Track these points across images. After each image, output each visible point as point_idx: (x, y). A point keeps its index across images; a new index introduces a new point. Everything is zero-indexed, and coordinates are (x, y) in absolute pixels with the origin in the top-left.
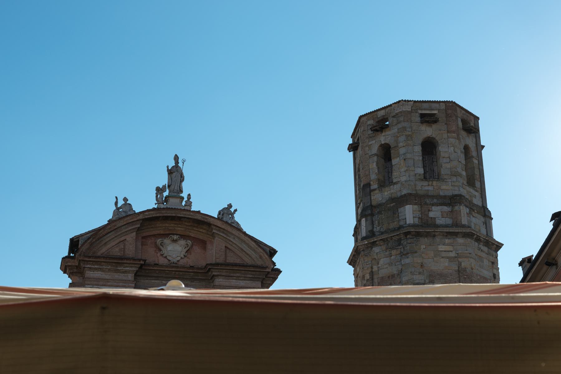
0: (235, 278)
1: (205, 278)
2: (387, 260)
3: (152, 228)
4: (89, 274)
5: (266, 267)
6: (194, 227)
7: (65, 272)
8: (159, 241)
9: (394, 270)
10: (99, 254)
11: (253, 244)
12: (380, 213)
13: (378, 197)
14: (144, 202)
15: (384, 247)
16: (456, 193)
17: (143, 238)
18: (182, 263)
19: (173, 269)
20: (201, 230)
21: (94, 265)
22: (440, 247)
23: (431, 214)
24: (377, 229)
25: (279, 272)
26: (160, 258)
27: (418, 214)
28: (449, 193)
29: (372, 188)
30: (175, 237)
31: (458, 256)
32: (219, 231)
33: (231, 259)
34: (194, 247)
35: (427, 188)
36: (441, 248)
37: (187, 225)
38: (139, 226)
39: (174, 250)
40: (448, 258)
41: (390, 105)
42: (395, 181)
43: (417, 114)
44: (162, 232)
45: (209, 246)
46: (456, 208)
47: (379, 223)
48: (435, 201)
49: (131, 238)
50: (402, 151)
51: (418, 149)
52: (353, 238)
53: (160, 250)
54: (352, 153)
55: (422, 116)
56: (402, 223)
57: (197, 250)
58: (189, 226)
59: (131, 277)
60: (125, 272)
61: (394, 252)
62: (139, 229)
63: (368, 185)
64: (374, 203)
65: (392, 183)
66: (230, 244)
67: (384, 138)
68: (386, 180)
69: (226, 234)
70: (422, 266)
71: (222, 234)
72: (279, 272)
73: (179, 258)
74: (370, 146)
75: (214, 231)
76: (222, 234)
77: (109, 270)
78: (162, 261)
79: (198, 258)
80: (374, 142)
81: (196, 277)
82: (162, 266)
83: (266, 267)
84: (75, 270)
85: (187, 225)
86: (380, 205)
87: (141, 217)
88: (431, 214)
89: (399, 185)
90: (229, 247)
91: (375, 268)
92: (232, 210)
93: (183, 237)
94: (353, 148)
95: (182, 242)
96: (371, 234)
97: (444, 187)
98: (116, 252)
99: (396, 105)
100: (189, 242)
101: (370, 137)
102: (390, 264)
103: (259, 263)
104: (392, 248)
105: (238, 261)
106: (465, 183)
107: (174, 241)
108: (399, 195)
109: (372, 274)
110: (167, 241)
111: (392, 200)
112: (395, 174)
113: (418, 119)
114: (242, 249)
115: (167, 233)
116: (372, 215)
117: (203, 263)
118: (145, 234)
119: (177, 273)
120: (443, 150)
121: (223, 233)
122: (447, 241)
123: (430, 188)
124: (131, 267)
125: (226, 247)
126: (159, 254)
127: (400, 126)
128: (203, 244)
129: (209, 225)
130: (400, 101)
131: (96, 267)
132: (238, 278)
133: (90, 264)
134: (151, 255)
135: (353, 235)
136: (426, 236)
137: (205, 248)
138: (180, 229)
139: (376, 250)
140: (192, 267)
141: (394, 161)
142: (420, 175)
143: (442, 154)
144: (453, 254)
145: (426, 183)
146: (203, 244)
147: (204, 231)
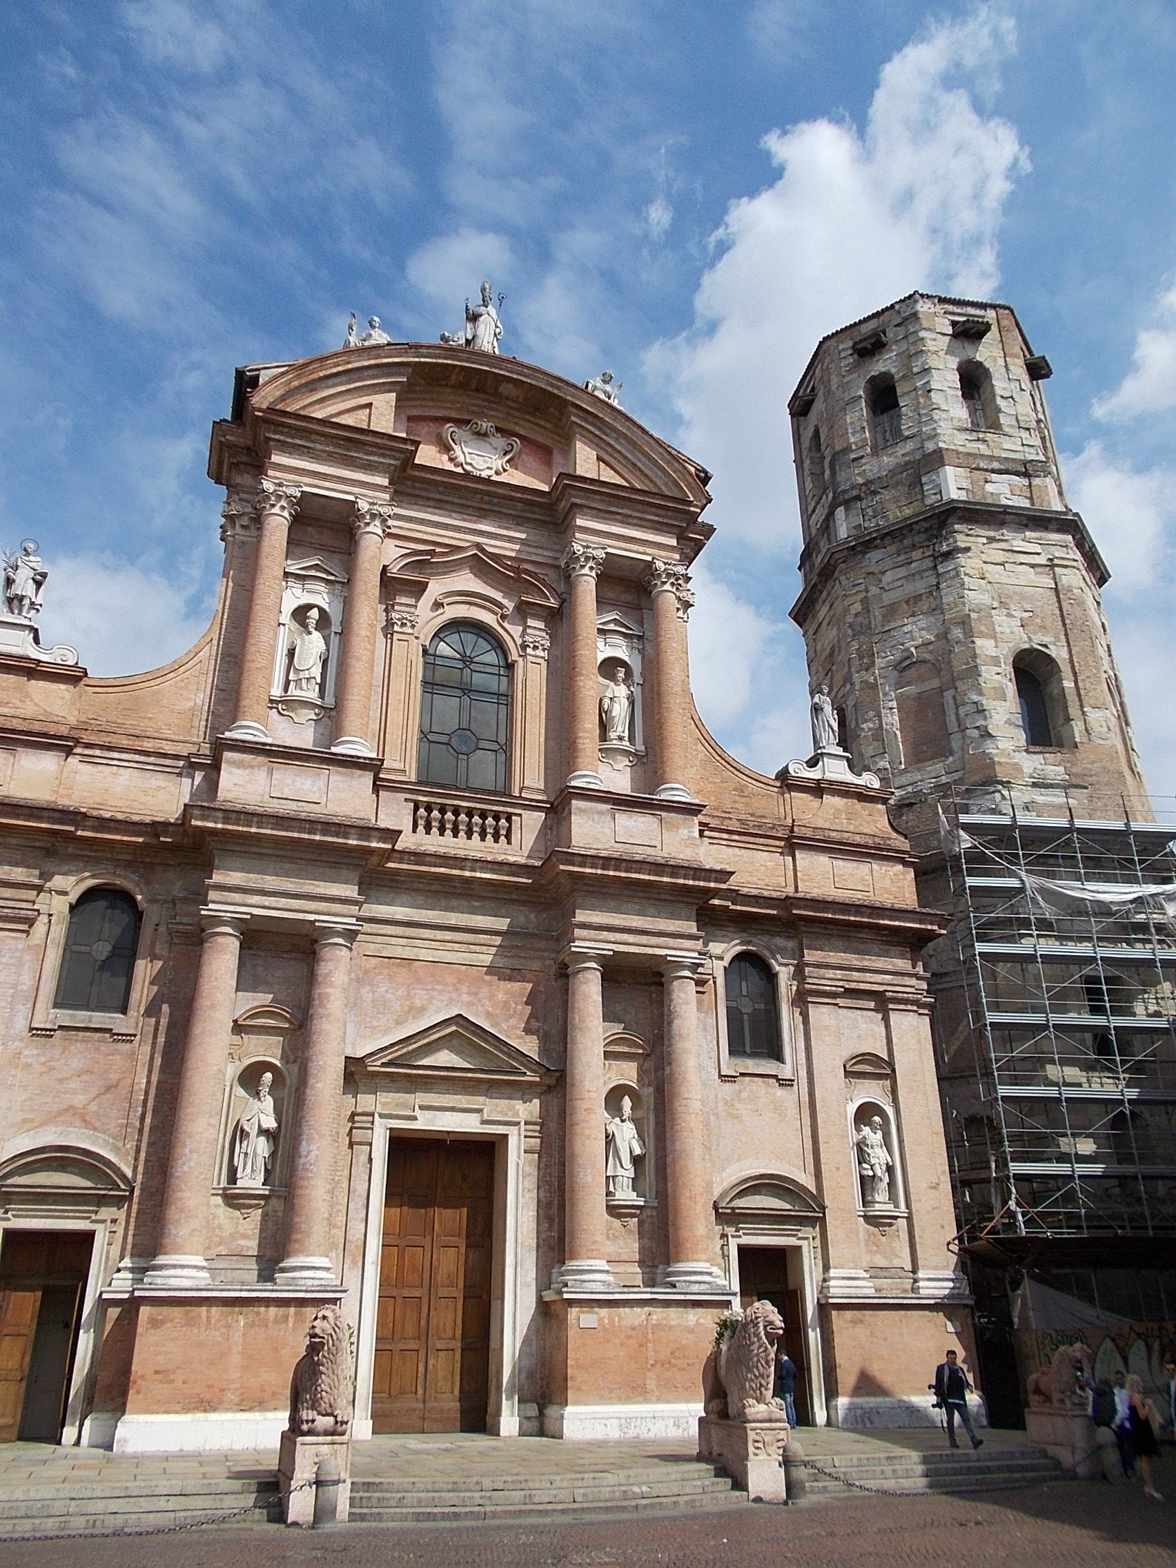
0: (619, 517)
1: (548, 519)
2: (902, 572)
3: (432, 400)
6: (528, 413)
7: (218, 482)
8: (449, 428)
9: (920, 586)
15: (892, 549)
19: (480, 487)
20: (542, 423)
21: (293, 438)
22: (1015, 543)
25: (709, 531)
30: (485, 425)
31: (1051, 565)
32: (586, 421)
34: (524, 456)
36: (1018, 544)
37: (511, 408)
40: (1033, 566)
42: (907, 433)
44: (454, 415)
45: (557, 457)
46: (1036, 481)
47: (874, 511)
48: (996, 465)
52: (799, 576)
55: (954, 324)
58: (516, 409)
60: (368, 467)
61: (916, 555)
66: (607, 452)
69: (599, 429)
71: (590, 427)
72: (709, 531)
73: (492, 472)
75: (573, 418)
76: (590, 427)
77: (330, 454)
81: (530, 515)
84: (244, 459)
85: (511, 408)
88: (989, 488)
89: (918, 438)
90: (606, 457)
91: (874, 590)
93: (498, 430)
94: (801, 407)
95: (500, 442)
99: (903, 305)
104: (914, 547)
107: (481, 435)
109: (865, 601)
110: (460, 433)
114: (634, 465)
115: (466, 417)
118: (415, 412)
119: (486, 498)
120: (1000, 385)
121: (594, 425)
124: (384, 456)
125: (599, 459)
126: (445, 457)
128: (544, 453)
129: (562, 404)
130: (910, 296)
131: (298, 442)
133: (281, 433)
135: (800, 568)
139: (874, 556)
142: (960, 420)
143: (998, 391)
144: (1042, 560)
147: (548, 425)
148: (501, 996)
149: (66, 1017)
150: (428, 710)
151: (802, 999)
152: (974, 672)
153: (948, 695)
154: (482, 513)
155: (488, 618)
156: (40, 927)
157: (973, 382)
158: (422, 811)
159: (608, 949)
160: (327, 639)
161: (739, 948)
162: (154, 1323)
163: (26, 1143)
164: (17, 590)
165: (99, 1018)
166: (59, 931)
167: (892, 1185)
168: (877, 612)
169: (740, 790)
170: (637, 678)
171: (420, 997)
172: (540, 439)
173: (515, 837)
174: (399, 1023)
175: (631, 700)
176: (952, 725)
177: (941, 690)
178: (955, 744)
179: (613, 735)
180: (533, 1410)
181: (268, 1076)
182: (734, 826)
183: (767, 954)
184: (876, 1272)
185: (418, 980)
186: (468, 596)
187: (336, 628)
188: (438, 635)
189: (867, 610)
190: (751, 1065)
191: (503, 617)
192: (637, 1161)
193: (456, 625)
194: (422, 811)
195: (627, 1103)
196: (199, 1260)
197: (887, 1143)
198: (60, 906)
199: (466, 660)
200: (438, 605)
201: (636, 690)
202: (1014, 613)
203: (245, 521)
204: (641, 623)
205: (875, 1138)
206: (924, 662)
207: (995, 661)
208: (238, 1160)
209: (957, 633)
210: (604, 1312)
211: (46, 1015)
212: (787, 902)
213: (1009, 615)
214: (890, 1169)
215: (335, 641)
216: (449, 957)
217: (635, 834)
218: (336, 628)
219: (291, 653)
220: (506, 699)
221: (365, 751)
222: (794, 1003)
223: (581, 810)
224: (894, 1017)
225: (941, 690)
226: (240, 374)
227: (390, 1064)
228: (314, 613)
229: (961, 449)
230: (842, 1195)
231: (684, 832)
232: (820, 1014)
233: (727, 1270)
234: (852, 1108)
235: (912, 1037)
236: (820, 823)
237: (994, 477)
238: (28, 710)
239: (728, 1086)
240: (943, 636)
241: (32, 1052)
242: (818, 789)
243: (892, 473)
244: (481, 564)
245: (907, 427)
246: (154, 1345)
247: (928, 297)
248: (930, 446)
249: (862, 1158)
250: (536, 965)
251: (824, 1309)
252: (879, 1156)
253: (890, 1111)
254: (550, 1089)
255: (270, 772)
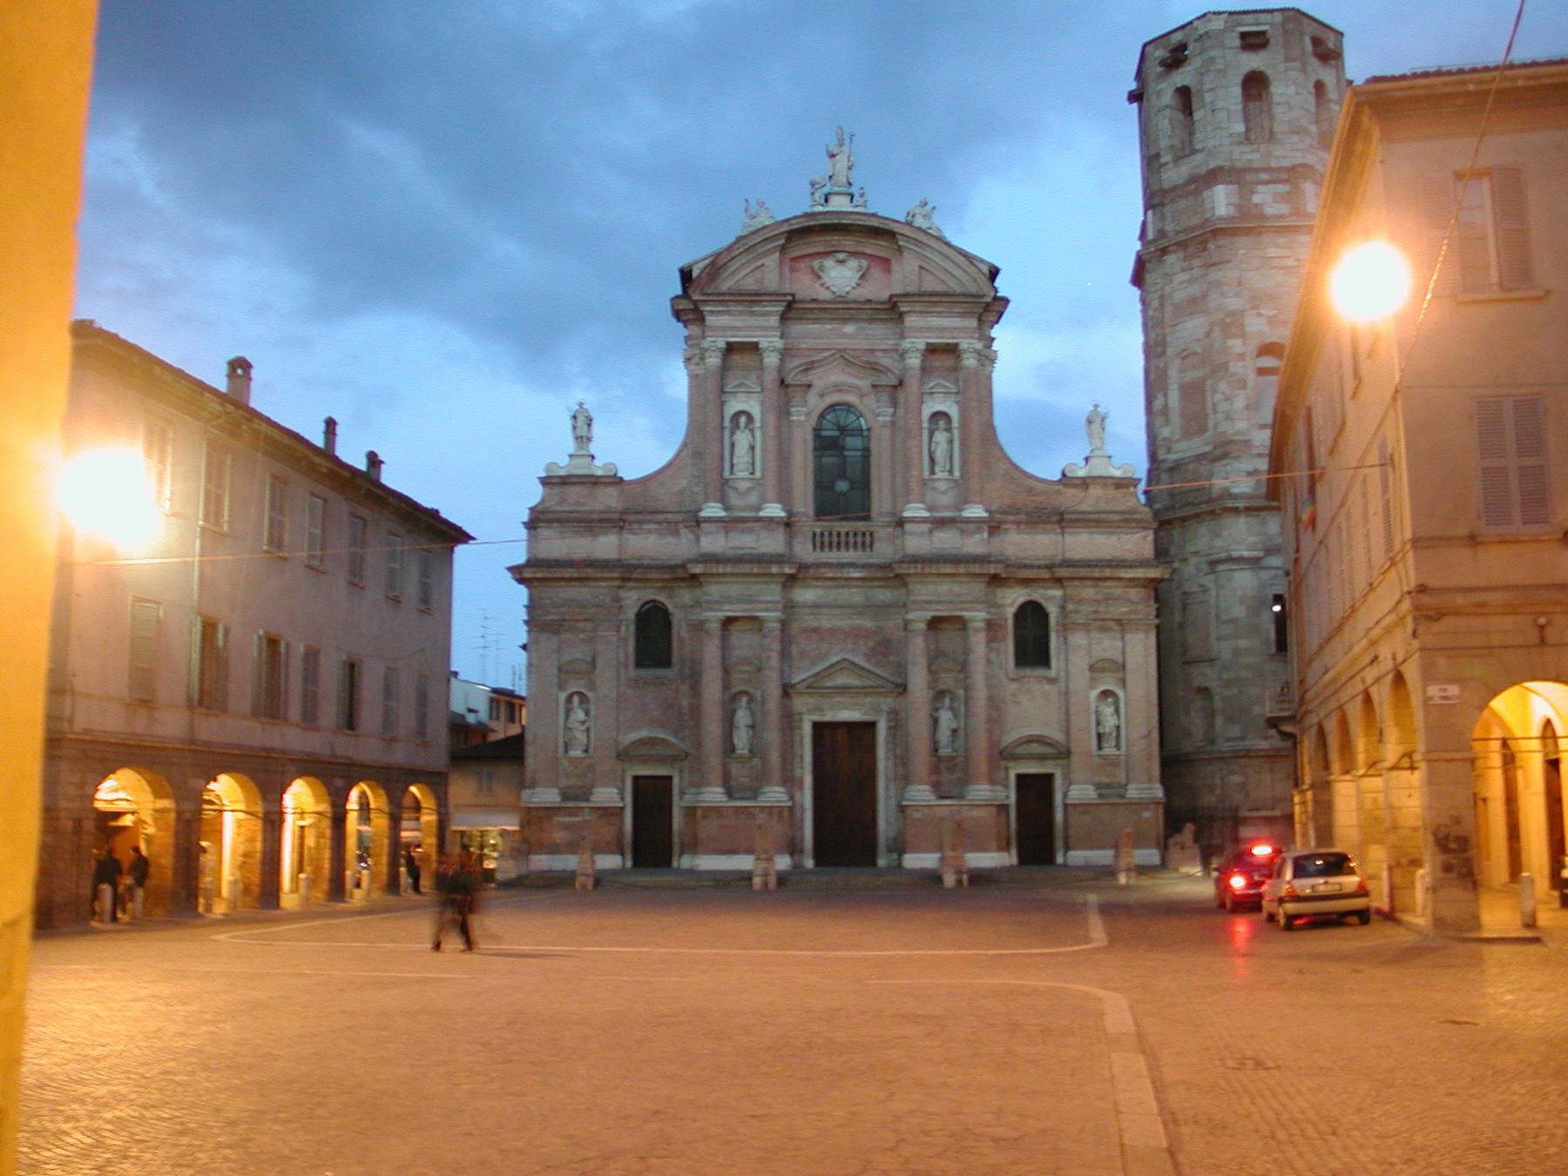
2: (1184, 276)
4: (711, 320)
5: (983, 296)
8: (816, 263)
9: (1195, 290)
10: (724, 288)
11: (961, 260)
12: (1173, 201)
13: (1174, 175)
14: (793, 203)
15: (1181, 254)
16: (1299, 161)
17: (793, 260)
18: (851, 297)
23: (1256, 199)
24: (1169, 228)
25: (1006, 301)
26: (821, 290)
27: (1235, 199)
28: (1287, 163)
29: (1163, 160)
30: (841, 256)
33: (930, 285)
35: (1250, 156)
38: (782, 242)
39: (840, 276)
41: (1191, 23)
43: (1236, 35)
44: (821, 249)
45: (895, 266)
49: (772, 261)
50: (1208, 98)
51: (1237, 91)
53: (819, 277)
54: (1135, 105)
55: (1244, 36)
56: (1208, 215)
57: (876, 272)
59: (774, 321)
60: (766, 314)
61: (1196, 262)
62: (783, 249)
63: (1158, 156)
64: (1166, 186)
65: (1194, 152)
67: (1181, 77)
68: (1186, 150)
70: (1240, 284)
72: (1006, 301)
74: (1159, 93)
78: (823, 295)
79: (878, 289)
80: (1164, 85)
82: (822, 302)
83: (983, 296)
86: (1175, 188)
87: (785, 228)
88: (1256, 199)
91: (1168, 289)
92: (928, 208)
93: (854, 254)
95: (853, 263)
96: (1161, 233)
97: (1277, 153)
98: (750, 284)
100: (865, 263)
101: (1160, 77)
102: (1191, 281)
103: (973, 289)
105: (940, 288)
106: (1315, 143)
107: (841, 262)
108: (1204, 170)
109: (1162, 297)
110: (829, 262)
111: (1193, 179)
112: (1198, 136)
113: (1238, 42)
116: (1162, 204)
117: (885, 296)
118: (794, 255)
122: (1281, 240)
123: (1254, 156)
127: (1205, 56)
128: (885, 263)
132: (940, 314)
134: (804, 286)
136: (1247, 234)
137: (888, 270)
138: (848, 243)
140: (869, 301)
141: (1198, 115)
143: (1276, 99)
145: (1248, 148)
146: (885, 263)
148: (871, 644)
149: (642, 672)
150: (819, 469)
151: (1065, 628)
152: (1225, 365)
153: (1209, 382)
154: (845, 321)
155: (851, 398)
156: (623, 628)
157: (1255, 84)
158: (818, 539)
159: (929, 614)
160: (752, 431)
161: (1022, 600)
162: (705, 817)
163: (635, 736)
164: (579, 433)
165: (660, 672)
166: (632, 628)
167: (1118, 737)
168: (1168, 309)
169: (1030, 490)
170: (955, 424)
171: (824, 647)
172: (882, 254)
173: (877, 546)
174: (814, 664)
175: (951, 442)
176: (1210, 410)
177: (1204, 379)
178: (1210, 424)
179: (937, 469)
180: (895, 856)
181: (744, 699)
182: (1022, 517)
183: (1042, 601)
184: (1099, 786)
185: (823, 639)
186: (838, 388)
187: (758, 424)
188: (822, 416)
189: (1162, 306)
190: (1028, 672)
191: (862, 396)
192: (954, 731)
193: (832, 407)
194: (818, 539)
195: (947, 701)
196: (720, 790)
197: (1117, 711)
198: (631, 614)
199: (843, 430)
200: (822, 396)
201: (956, 432)
202: (1263, 312)
203: (696, 359)
204: (956, 382)
205: (1108, 710)
206: (1195, 354)
207: (1242, 357)
208: (736, 741)
209: (1217, 333)
210: (926, 811)
211: (632, 673)
212: (1049, 567)
213: (1259, 315)
214: (1118, 728)
215: (758, 434)
216: (839, 623)
217: (946, 541)
218: (758, 424)
219: (733, 445)
220: (866, 452)
221: (775, 510)
222: (1058, 632)
223: (913, 533)
224: (1128, 637)
225: (1204, 379)
226: (682, 271)
227: (809, 687)
228: (743, 420)
229: (1239, 165)
230: (1084, 742)
231: (977, 537)
232: (1078, 639)
233: (1007, 787)
234: (1095, 693)
235: (1140, 650)
236: (1084, 507)
237: (1261, 188)
238: (598, 506)
239: (1013, 687)
240: (1208, 334)
241: (630, 692)
242: (1084, 483)
243: (1187, 183)
244: (846, 358)
245: (1199, 140)
246: (707, 828)
247: (1219, 13)
248: (1212, 165)
249: (1098, 724)
250: (891, 623)
251: (1066, 806)
252: (1110, 722)
253: (1120, 693)
254: (900, 694)
255: (727, 532)
